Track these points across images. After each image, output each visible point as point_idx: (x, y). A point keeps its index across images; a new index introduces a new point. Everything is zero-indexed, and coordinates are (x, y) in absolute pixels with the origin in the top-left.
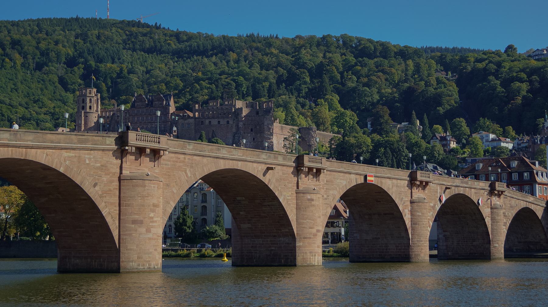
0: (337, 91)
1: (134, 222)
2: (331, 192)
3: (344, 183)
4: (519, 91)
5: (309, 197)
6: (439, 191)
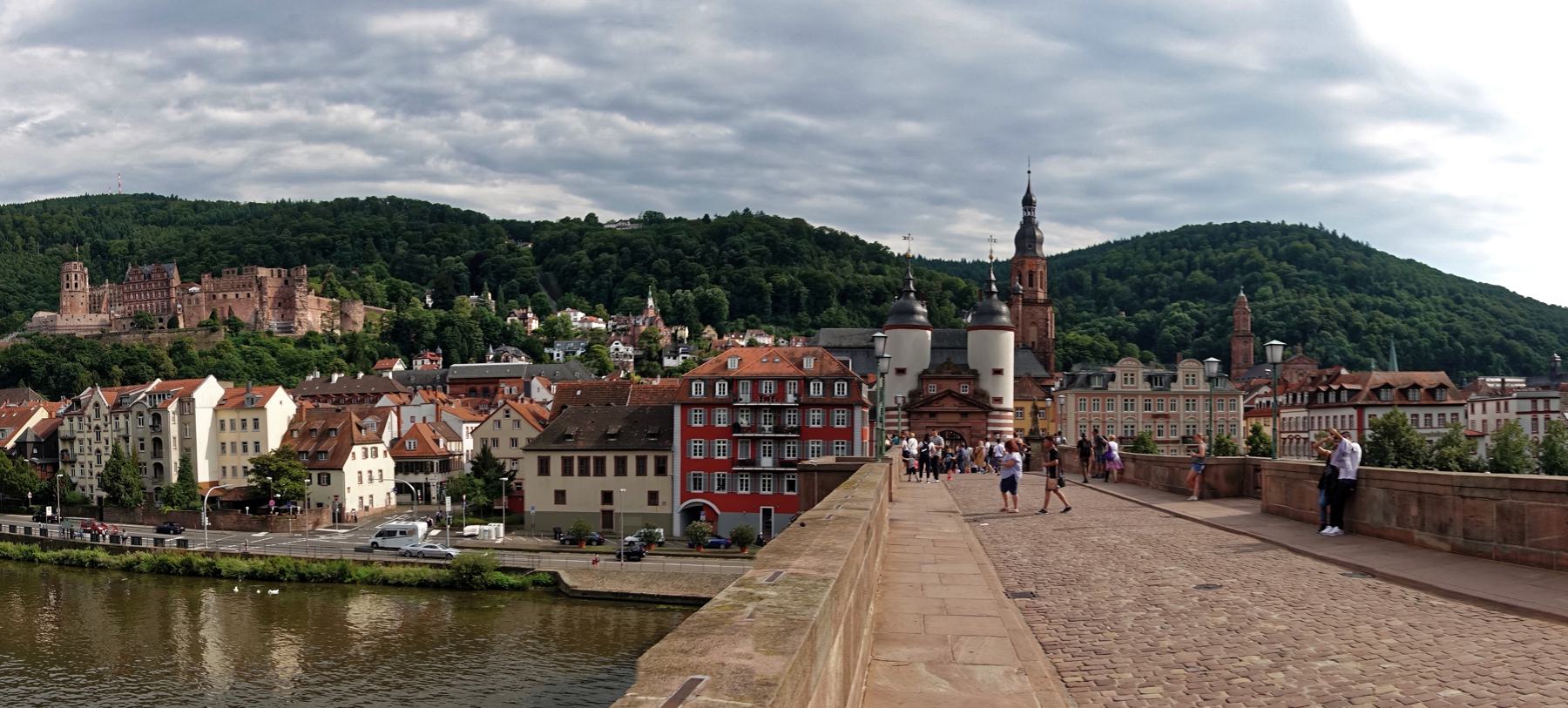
4: (609, 262)
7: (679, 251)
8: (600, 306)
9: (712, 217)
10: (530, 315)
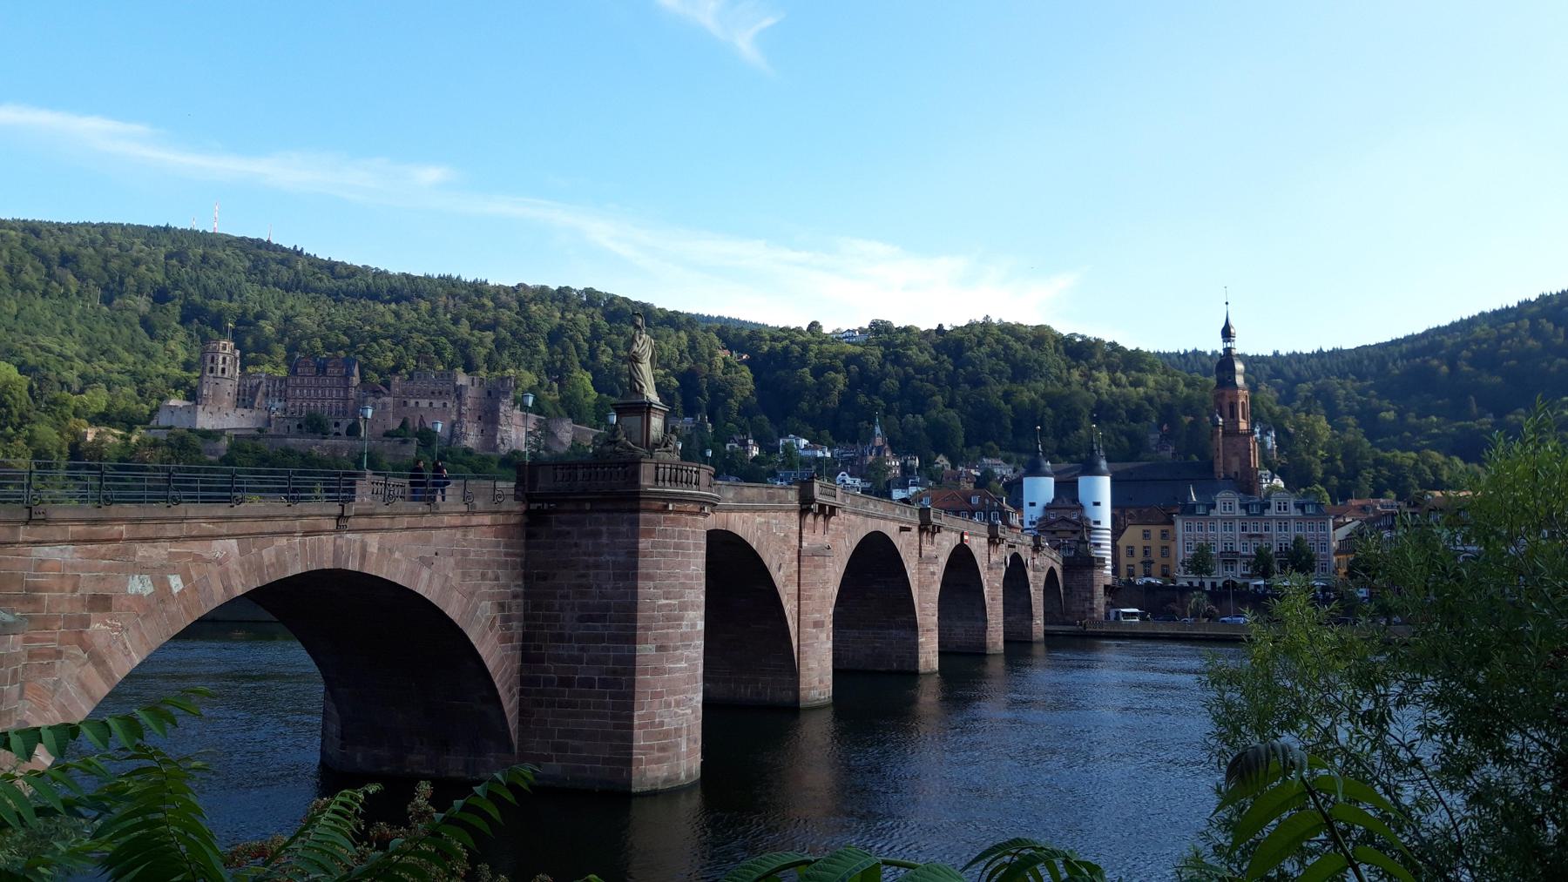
0: (584, 366)
7: (911, 370)
8: (826, 433)
9: (947, 328)
10: (751, 442)
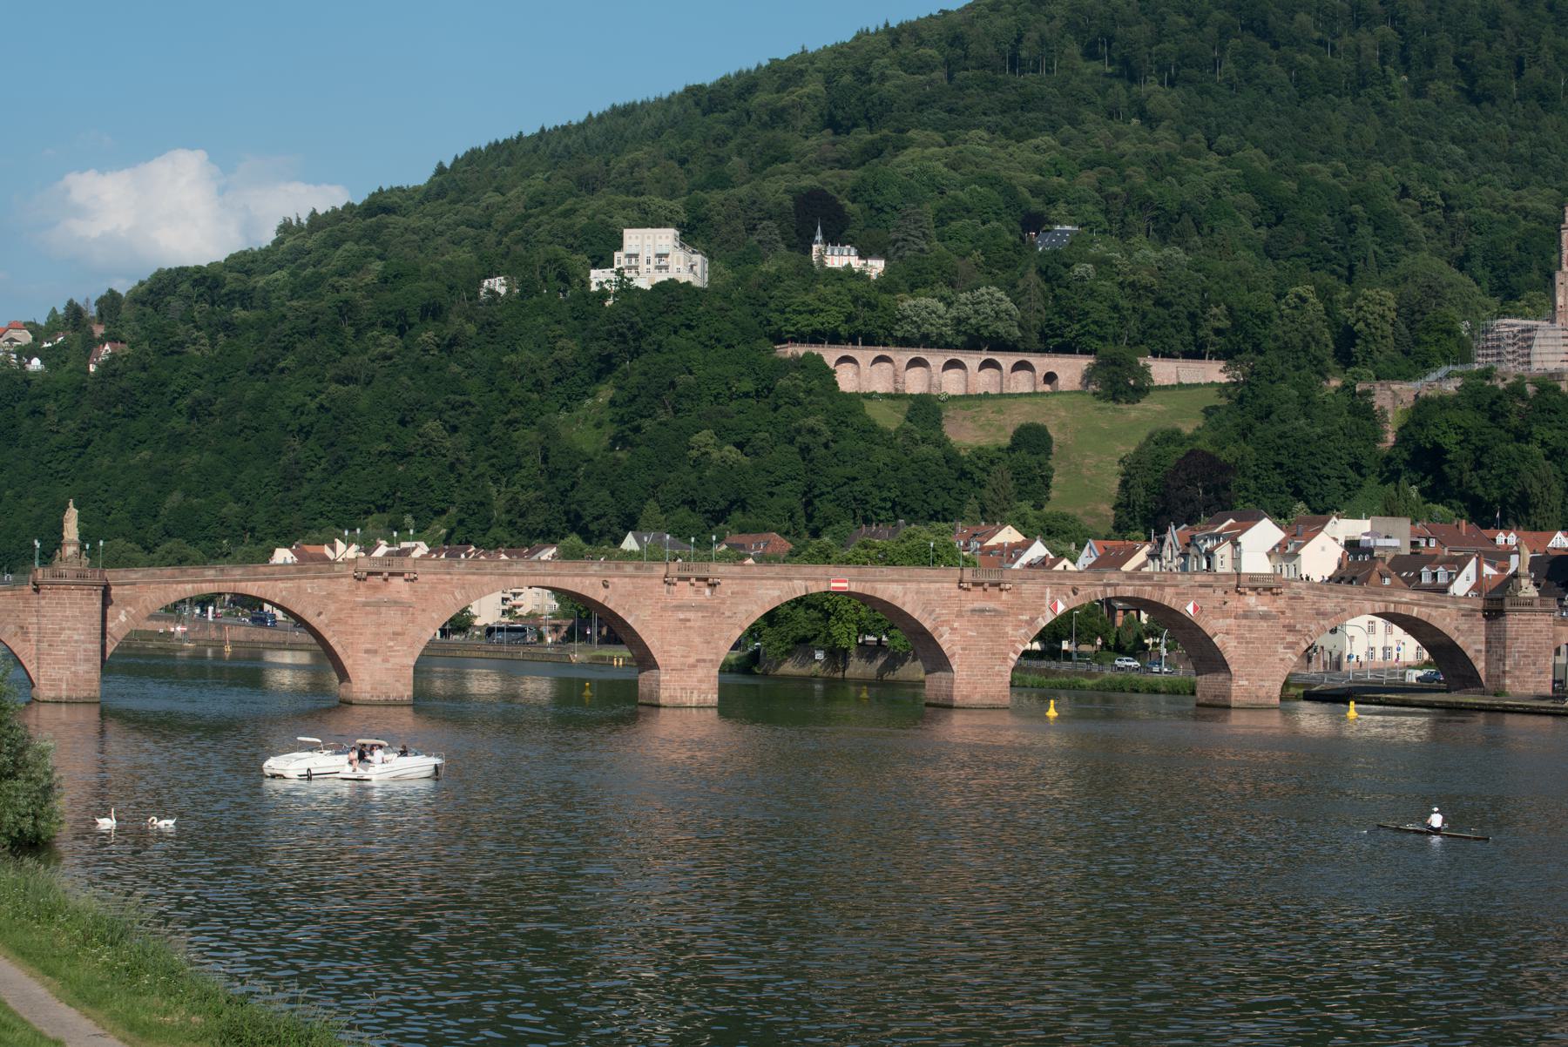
1: (367, 651)
2: (742, 608)
3: (777, 593)
5: (682, 616)
6: (1048, 596)
